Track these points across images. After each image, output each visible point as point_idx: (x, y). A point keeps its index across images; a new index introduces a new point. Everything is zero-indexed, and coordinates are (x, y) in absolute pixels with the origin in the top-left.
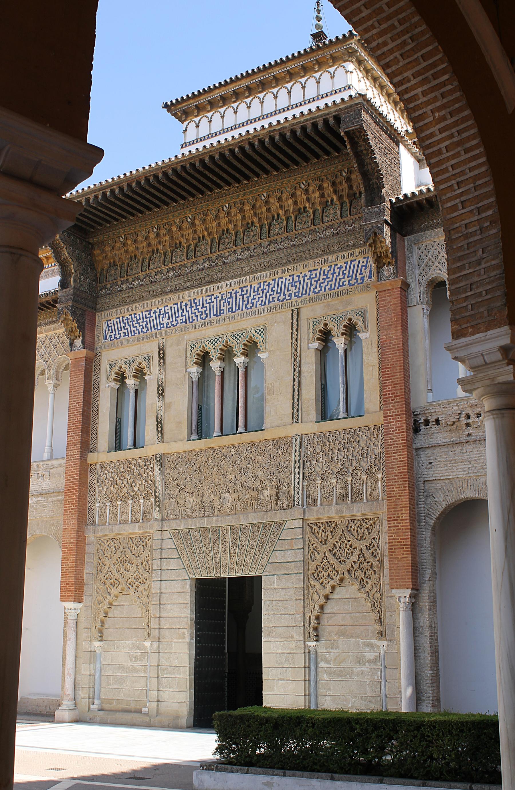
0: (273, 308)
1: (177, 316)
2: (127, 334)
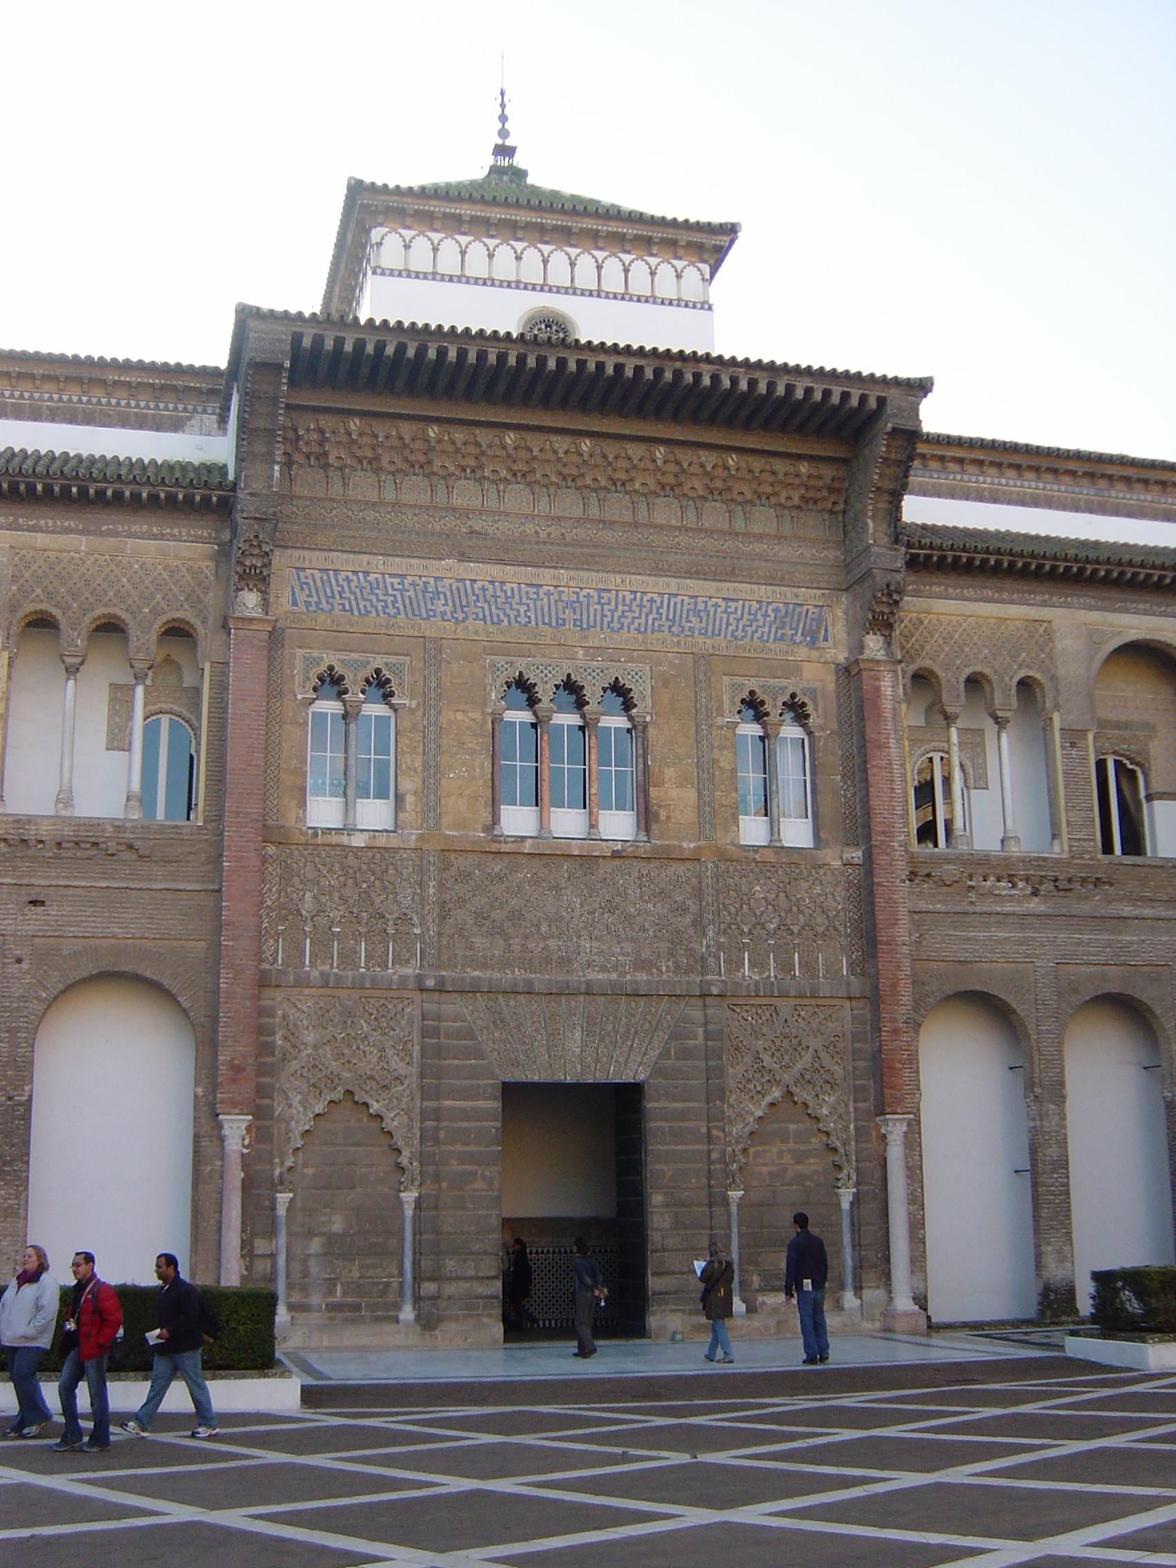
1: (464, 603)
2: (347, 607)
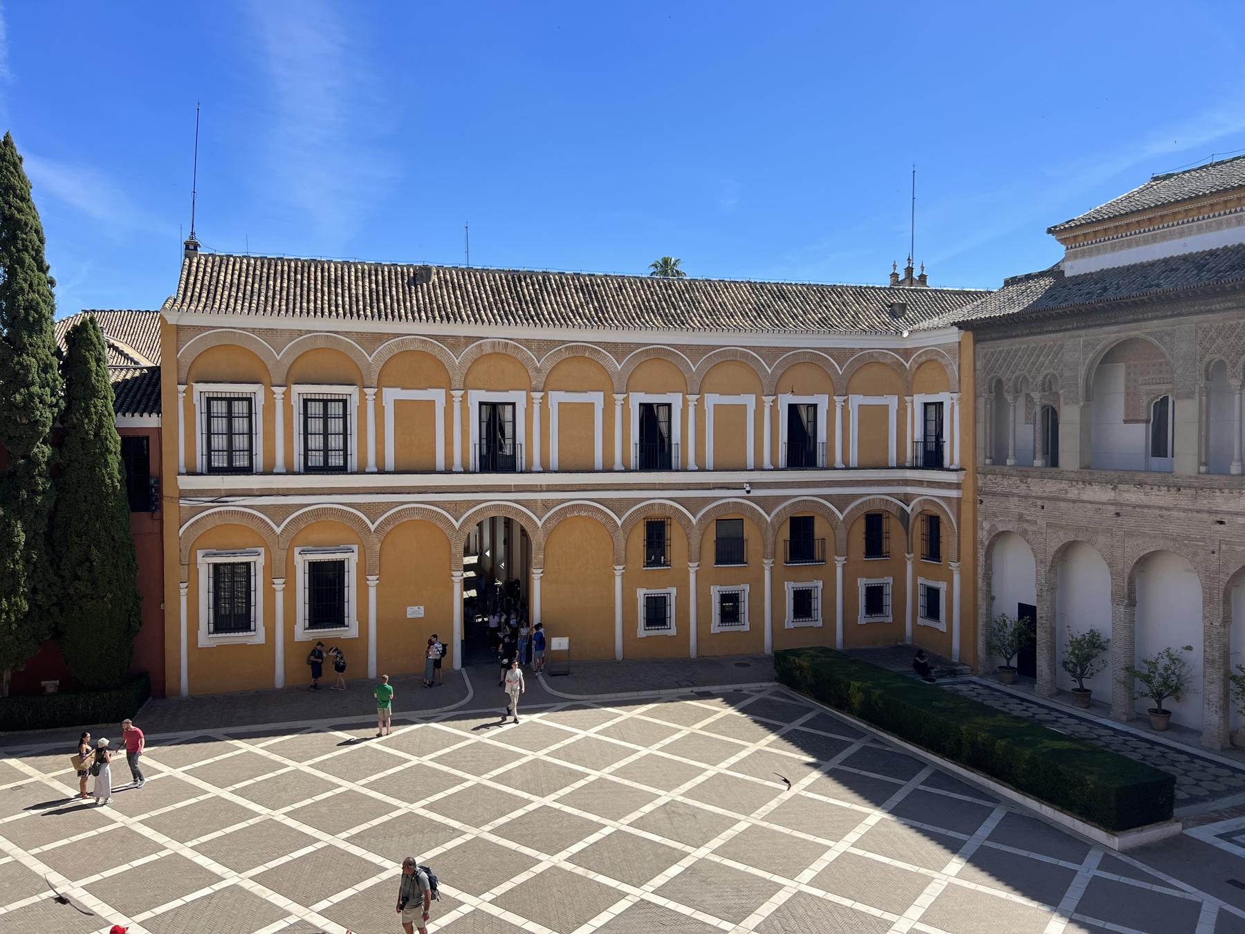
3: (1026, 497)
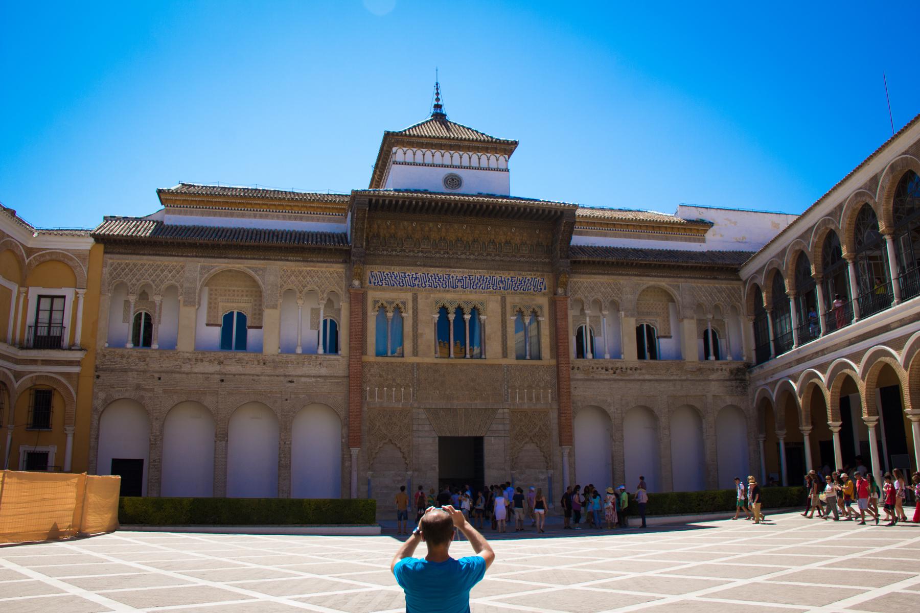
0: (490, 292)
3: (145, 372)
